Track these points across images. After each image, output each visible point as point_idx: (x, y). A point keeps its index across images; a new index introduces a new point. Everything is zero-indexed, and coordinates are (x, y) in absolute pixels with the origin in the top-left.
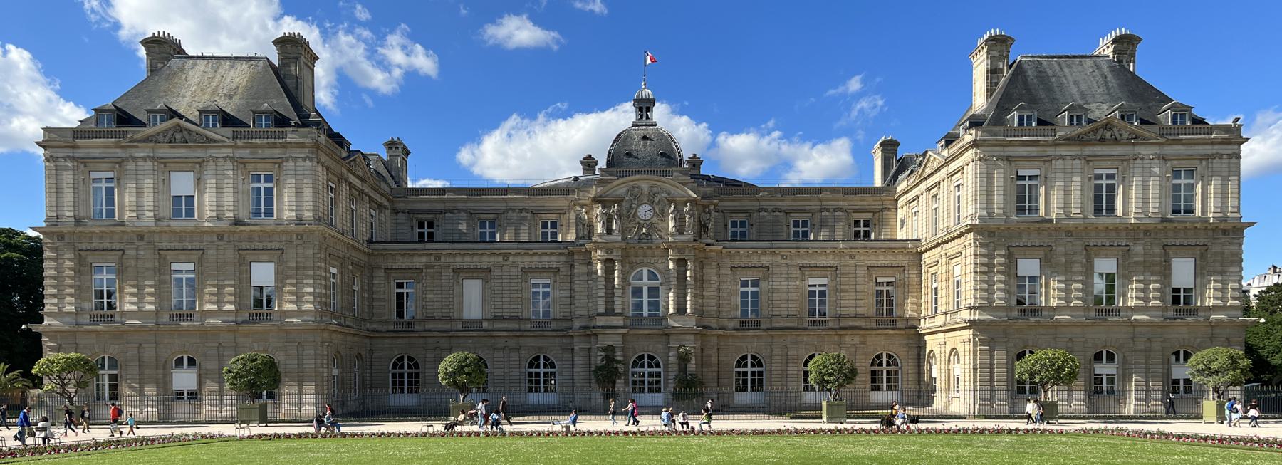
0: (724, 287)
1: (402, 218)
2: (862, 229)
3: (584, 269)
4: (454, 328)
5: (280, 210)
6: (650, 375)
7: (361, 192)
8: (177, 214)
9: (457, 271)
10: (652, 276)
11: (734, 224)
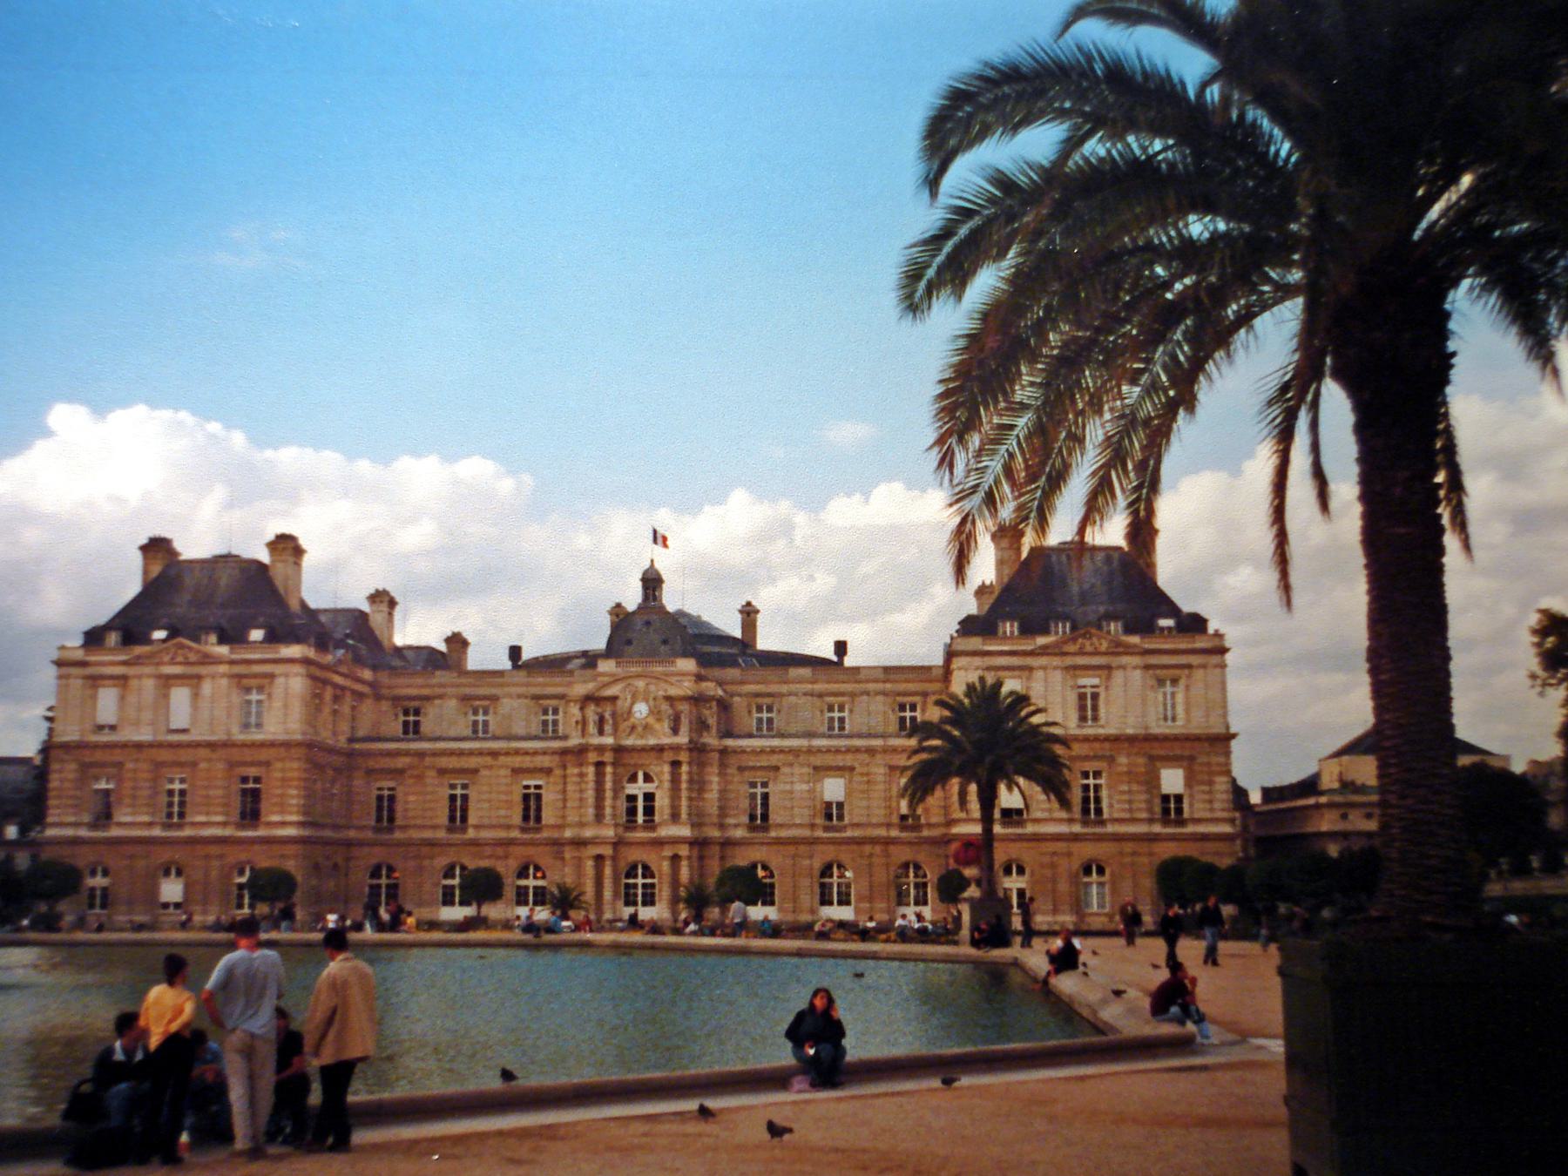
1: (385, 706)
3: (576, 771)
6: (644, 886)
7: (343, 688)
9: (442, 772)
10: (648, 779)
11: (760, 709)
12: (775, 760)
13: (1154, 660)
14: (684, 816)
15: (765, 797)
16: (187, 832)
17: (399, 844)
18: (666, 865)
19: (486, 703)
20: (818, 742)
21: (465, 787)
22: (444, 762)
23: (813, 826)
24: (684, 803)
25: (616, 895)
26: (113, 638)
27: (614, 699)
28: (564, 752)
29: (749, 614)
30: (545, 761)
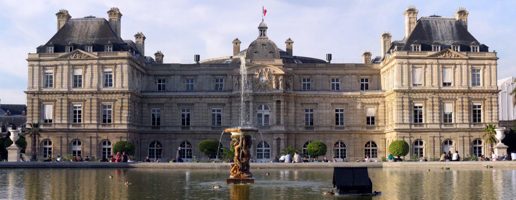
0: (298, 112)
1: (151, 78)
2: (365, 83)
4: (178, 130)
5: (115, 84)
9: (179, 104)
10: (266, 108)
11: (304, 80)
12: (316, 100)
13: (471, 62)
14: (281, 123)
15: (312, 115)
16: (82, 127)
17: (163, 133)
18: (275, 143)
19: (192, 77)
20: (332, 93)
21: (188, 110)
22: (180, 101)
24: (282, 118)
25: (254, 154)
26: (51, 49)
28: (231, 97)
29: (289, 42)
30: (223, 101)
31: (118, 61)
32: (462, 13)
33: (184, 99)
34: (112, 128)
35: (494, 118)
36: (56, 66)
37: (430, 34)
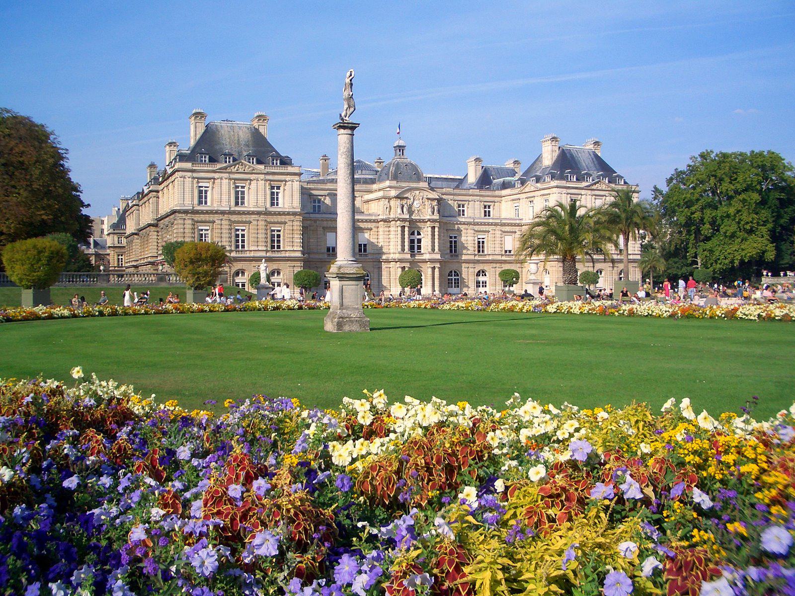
3: (388, 229)
8: (237, 204)
15: (455, 242)
18: (430, 270)
23: (475, 255)
27: (407, 198)
31: (288, 178)
32: (596, 143)
33: (330, 222)
34: (283, 255)
35: (636, 249)
36: (214, 179)
37: (576, 164)
